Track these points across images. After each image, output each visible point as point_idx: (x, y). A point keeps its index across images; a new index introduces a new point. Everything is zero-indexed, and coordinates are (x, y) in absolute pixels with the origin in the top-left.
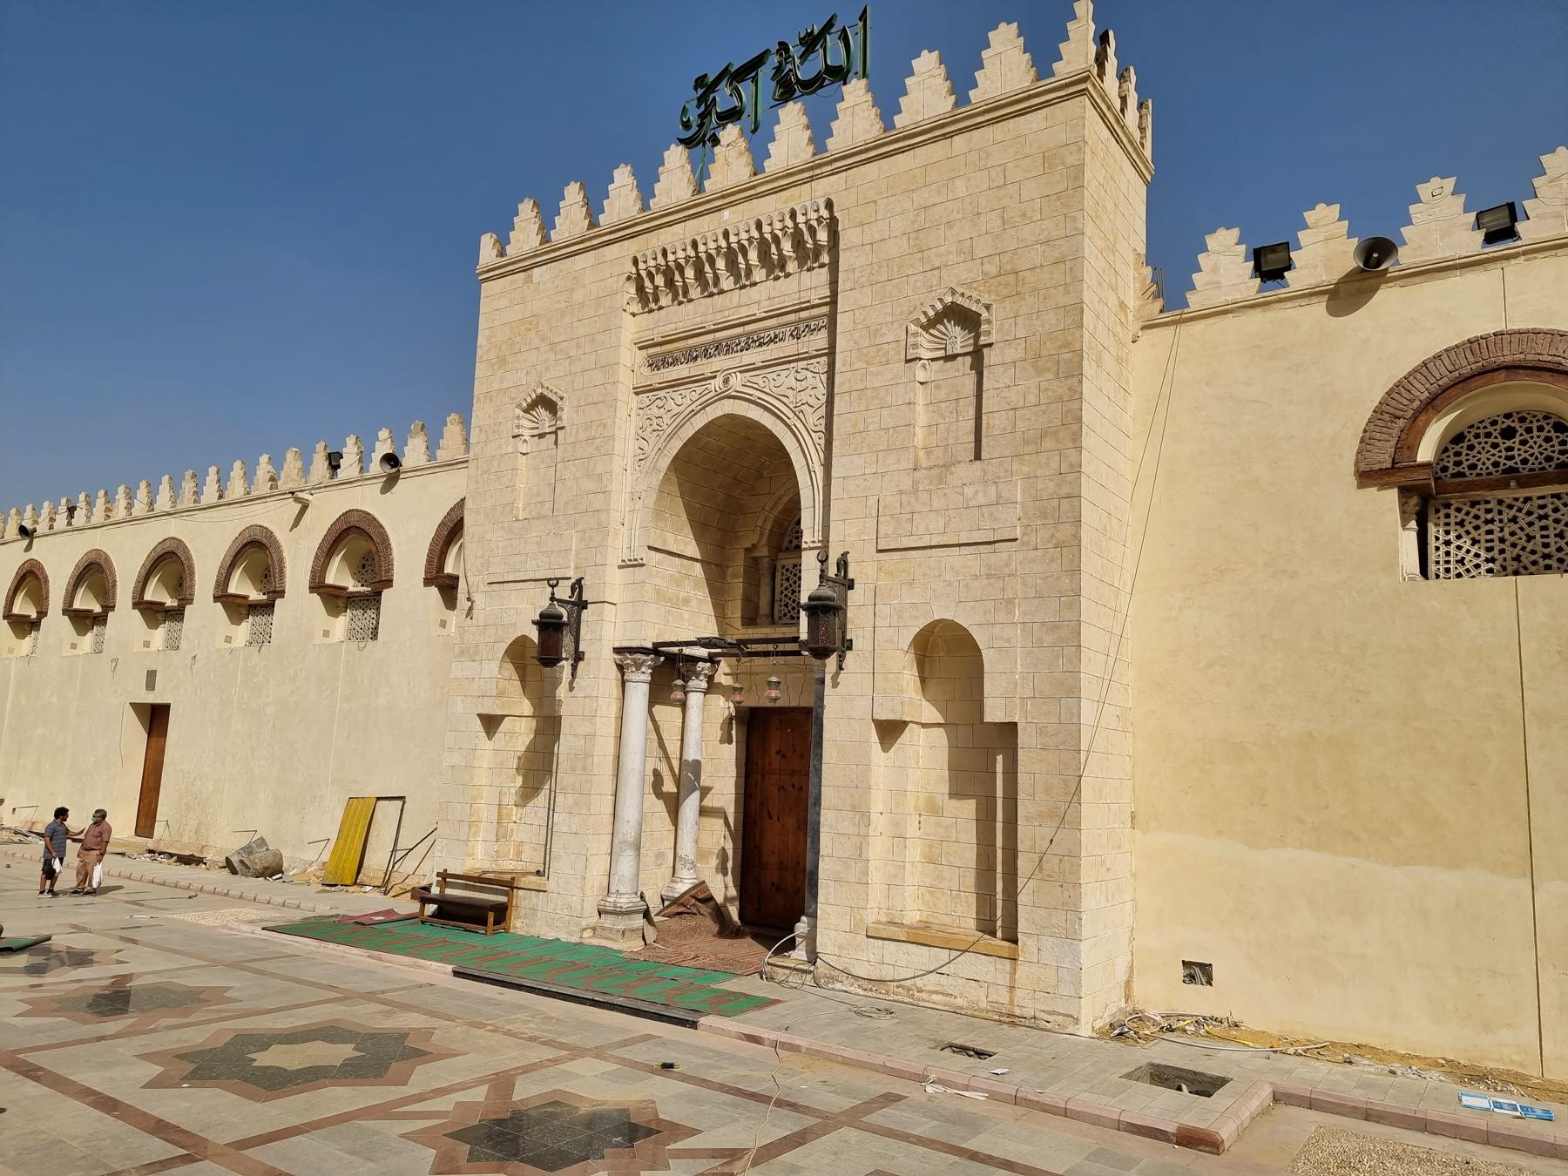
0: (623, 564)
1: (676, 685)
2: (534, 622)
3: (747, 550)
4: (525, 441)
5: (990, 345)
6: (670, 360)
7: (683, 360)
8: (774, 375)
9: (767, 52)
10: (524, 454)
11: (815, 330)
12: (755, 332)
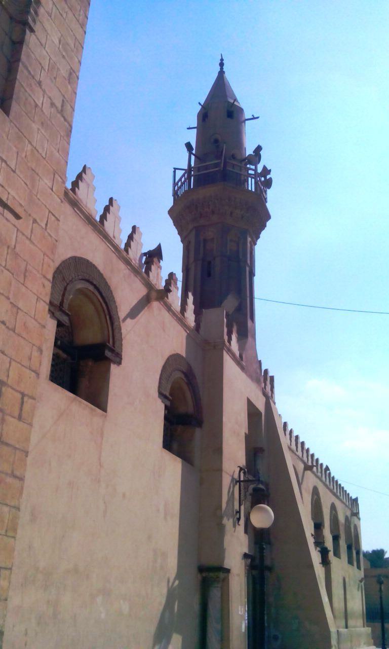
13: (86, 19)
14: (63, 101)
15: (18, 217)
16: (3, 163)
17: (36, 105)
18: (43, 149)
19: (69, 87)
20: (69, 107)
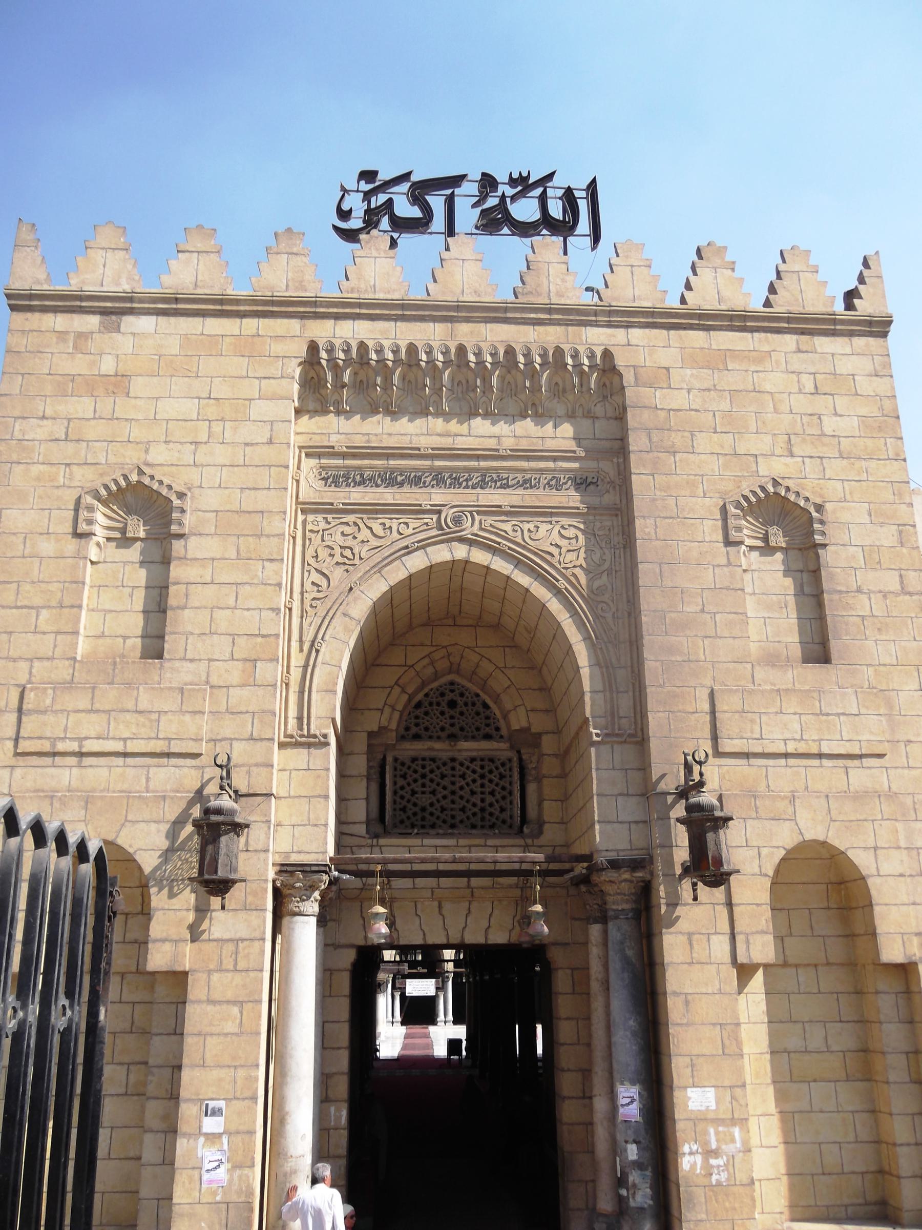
0: (288, 740)
1: (377, 914)
3: (371, 735)
4: (98, 544)
5: (825, 546)
6: (358, 478)
7: (379, 482)
8: (531, 526)
9: (462, 177)
10: (92, 563)
11: (581, 484)
12: (496, 469)
13: (899, 442)
14: (901, 576)
15: (881, 756)
16: (842, 717)
17: (863, 617)
18: (891, 655)
19: (904, 550)
20: (912, 573)
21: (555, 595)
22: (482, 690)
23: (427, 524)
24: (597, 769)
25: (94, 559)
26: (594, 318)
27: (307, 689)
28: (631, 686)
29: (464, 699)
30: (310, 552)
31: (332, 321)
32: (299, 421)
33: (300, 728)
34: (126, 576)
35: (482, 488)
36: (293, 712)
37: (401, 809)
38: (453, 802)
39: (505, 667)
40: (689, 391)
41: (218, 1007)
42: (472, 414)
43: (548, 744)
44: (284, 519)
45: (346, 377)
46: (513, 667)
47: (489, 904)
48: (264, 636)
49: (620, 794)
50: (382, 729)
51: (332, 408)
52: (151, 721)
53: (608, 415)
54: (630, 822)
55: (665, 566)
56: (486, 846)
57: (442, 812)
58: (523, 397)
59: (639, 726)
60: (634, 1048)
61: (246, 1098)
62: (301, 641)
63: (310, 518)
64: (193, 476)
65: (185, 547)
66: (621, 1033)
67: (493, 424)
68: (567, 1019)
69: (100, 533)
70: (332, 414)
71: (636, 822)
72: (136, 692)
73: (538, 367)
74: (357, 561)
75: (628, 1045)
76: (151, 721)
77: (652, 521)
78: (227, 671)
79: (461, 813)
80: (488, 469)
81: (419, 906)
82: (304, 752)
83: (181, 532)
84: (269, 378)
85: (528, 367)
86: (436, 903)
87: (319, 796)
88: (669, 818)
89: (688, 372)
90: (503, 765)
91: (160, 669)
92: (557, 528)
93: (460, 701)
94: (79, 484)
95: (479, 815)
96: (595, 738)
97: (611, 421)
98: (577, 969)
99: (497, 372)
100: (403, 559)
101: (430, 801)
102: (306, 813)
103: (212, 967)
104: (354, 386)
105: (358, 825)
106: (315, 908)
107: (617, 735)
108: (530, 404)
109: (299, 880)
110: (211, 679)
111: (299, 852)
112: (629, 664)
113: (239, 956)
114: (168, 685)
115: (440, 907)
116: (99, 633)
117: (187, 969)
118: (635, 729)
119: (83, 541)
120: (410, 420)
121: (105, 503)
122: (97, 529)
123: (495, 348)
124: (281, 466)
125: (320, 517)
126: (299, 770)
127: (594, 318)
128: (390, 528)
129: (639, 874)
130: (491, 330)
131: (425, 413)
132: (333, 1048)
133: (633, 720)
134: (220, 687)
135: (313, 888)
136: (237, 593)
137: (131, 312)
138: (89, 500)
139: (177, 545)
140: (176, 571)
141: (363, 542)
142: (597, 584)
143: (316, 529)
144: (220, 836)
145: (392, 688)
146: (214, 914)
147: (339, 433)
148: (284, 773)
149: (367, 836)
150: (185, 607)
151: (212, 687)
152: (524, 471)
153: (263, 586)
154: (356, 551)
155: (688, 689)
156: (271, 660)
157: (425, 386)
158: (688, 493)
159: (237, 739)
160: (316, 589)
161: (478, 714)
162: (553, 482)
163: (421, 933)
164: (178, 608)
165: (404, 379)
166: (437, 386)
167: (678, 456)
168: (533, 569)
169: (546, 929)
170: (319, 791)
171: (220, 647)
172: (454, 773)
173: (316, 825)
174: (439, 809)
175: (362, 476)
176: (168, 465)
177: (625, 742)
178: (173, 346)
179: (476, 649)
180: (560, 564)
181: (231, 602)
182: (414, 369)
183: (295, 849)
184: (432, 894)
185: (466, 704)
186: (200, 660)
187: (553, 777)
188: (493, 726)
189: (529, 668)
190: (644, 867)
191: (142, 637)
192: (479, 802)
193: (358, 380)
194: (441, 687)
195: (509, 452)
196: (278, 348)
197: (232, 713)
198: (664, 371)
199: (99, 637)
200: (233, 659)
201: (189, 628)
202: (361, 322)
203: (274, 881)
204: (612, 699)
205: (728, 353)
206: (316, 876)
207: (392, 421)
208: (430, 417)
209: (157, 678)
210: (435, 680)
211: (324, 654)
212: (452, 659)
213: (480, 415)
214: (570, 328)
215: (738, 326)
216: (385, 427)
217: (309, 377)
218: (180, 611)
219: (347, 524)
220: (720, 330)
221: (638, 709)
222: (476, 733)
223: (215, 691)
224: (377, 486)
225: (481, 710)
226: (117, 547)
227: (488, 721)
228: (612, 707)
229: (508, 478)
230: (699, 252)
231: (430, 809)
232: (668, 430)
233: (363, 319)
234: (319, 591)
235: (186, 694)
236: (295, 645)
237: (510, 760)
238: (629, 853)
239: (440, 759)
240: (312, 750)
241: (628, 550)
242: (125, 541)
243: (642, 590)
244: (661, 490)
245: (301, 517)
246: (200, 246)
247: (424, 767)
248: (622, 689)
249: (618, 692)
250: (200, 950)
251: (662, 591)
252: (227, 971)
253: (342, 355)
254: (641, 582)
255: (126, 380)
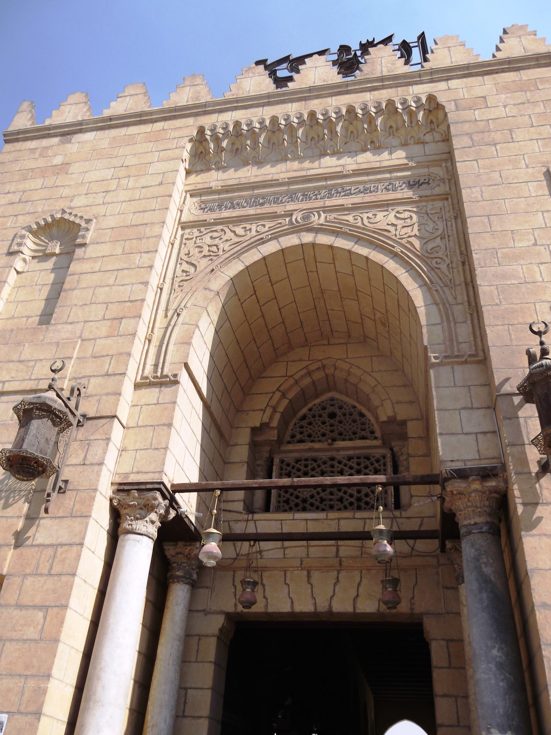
2: (368, 40)
3: (254, 431)
7: (245, 205)
8: (370, 215)
10: (18, 273)
11: (414, 185)
12: (341, 184)
21: (392, 258)
22: (358, 401)
23: (280, 223)
24: (437, 387)
25: (19, 269)
26: (419, 79)
27: (165, 342)
28: (468, 315)
29: (343, 410)
30: (184, 251)
31: (217, 114)
32: (189, 178)
33: (155, 371)
34: (40, 279)
35: (328, 198)
36: (151, 360)
37: (284, 502)
38: (331, 494)
39: (372, 372)
40: (505, 107)
41: (24, 612)
42: (324, 154)
43: (413, 429)
44: (163, 227)
45: (224, 144)
46: (379, 371)
47: (357, 574)
48: (131, 301)
49: (464, 408)
50: (264, 427)
51: (213, 167)
52: (28, 367)
53: (436, 139)
54: (476, 433)
55: (492, 218)
56: (354, 518)
57: (321, 503)
58: (362, 137)
59: (480, 347)
60: (501, 684)
61: (30, 713)
62: (167, 310)
63: (187, 231)
64: (101, 210)
65: (85, 252)
66: (483, 666)
67: (338, 159)
68: (444, 696)
69: (27, 253)
70: (214, 171)
71: (484, 433)
72: (22, 347)
73: (374, 114)
74: (221, 253)
75: (493, 681)
76: (28, 367)
77: (478, 189)
78: (97, 328)
79: (339, 503)
80: (334, 185)
81: (289, 575)
82: (156, 390)
83: (84, 242)
84: (166, 150)
85: (366, 116)
86: (305, 573)
87: (164, 425)
88: (518, 418)
89: (503, 96)
90: (378, 461)
91: (45, 331)
92: (393, 214)
93: (339, 412)
94: (20, 225)
95: (356, 505)
96: (433, 360)
97: (439, 143)
98: (453, 640)
99: (341, 124)
100: (259, 247)
101: (310, 494)
102: (150, 440)
103: (28, 571)
104: (232, 151)
105: (236, 503)
106: (153, 531)
107: (457, 356)
108: (369, 142)
109: (134, 499)
110: (83, 335)
111: (138, 473)
112: (466, 298)
113: (56, 560)
114: (49, 341)
115: (309, 576)
116: (11, 316)
117: (4, 572)
118: (476, 350)
119: (13, 257)
120: (272, 166)
121: (34, 233)
122: (24, 249)
123: (339, 109)
124: (166, 196)
125: (195, 230)
126: (148, 405)
127: (419, 79)
128: (250, 229)
129: (492, 483)
130: (335, 100)
131: (285, 159)
132: (194, 717)
133: (473, 342)
134: (90, 339)
135: (149, 508)
136: (117, 276)
137: (81, 131)
138: (24, 232)
139: (79, 252)
140: (74, 267)
141: (227, 240)
142: (430, 246)
143: (190, 237)
144: (32, 418)
145: (274, 393)
146: (42, 521)
147: (217, 180)
148: (136, 408)
149: (244, 512)
150: (75, 289)
151: (82, 340)
152: (364, 182)
153: (138, 269)
154: (221, 246)
155: (527, 305)
156: (135, 317)
157: (284, 139)
158: (510, 167)
159: (94, 376)
160: (185, 274)
161: (354, 421)
162: (390, 187)
163: (289, 601)
164: (70, 290)
165: (269, 142)
166: (294, 140)
167: (498, 147)
168: (371, 243)
169: (389, 549)
170: (164, 421)
171: (97, 312)
172: (333, 469)
173: (157, 449)
174: (319, 500)
175: (232, 203)
176: (84, 207)
177: (466, 362)
178: (105, 144)
179: (347, 360)
180: (396, 235)
181: (111, 282)
182: (277, 133)
183: (135, 470)
184: (301, 564)
185: (344, 415)
186: (78, 322)
187: (420, 456)
188: (368, 430)
189: (393, 370)
190: (496, 475)
191: (41, 316)
192: (355, 494)
193: (235, 148)
194: (323, 402)
195: (351, 172)
196: (176, 134)
197: (95, 357)
198: (482, 99)
199: (10, 318)
200: (104, 319)
201: (75, 302)
202: (238, 111)
203: (111, 500)
204: (450, 328)
205: (538, 80)
206: (151, 494)
207: (258, 169)
208: (288, 162)
209: (41, 338)
210: (317, 396)
211: (185, 317)
212: (327, 371)
213: (328, 155)
214: (399, 89)
215: (544, 63)
216: (253, 172)
217: (199, 152)
218: (71, 292)
219: (216, 231)
220: (529, 68)
221: (478, 333)
222: (353, 436)
223: (84, 342)
224: (243, 207)
225: (358, 418)
226: (38, 262)
227: (363, 427)
228: (451, 334)
229: (350, 189)
230: (505, 32)
231: (311, 501)
232: (488, 132)
233: (239, 109)
234: (187, 276)
235: (61, 345)
236: (161, 312)
237: (384, 457)
238: (477, 462)
239: (320, 459)
240: (163, 389)
241: (459, 221)
242: (45, 256)
243: (471, 237)
244: (484, 169)
245: (180, 232)
246: (132, 92)
247: (306, 466)
248: (459, 321)
249: (455, 323)
250: (22, 554)
251: (492, 234)
252: (41, 575)
253: (222, 131)
254: (470, 231)
255: (67, 166)
